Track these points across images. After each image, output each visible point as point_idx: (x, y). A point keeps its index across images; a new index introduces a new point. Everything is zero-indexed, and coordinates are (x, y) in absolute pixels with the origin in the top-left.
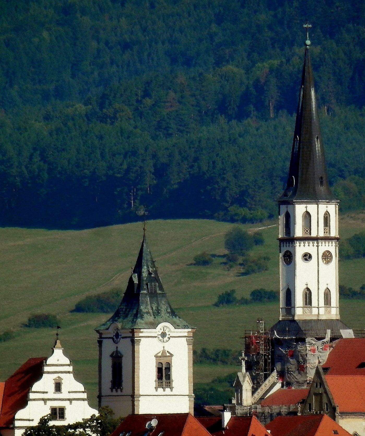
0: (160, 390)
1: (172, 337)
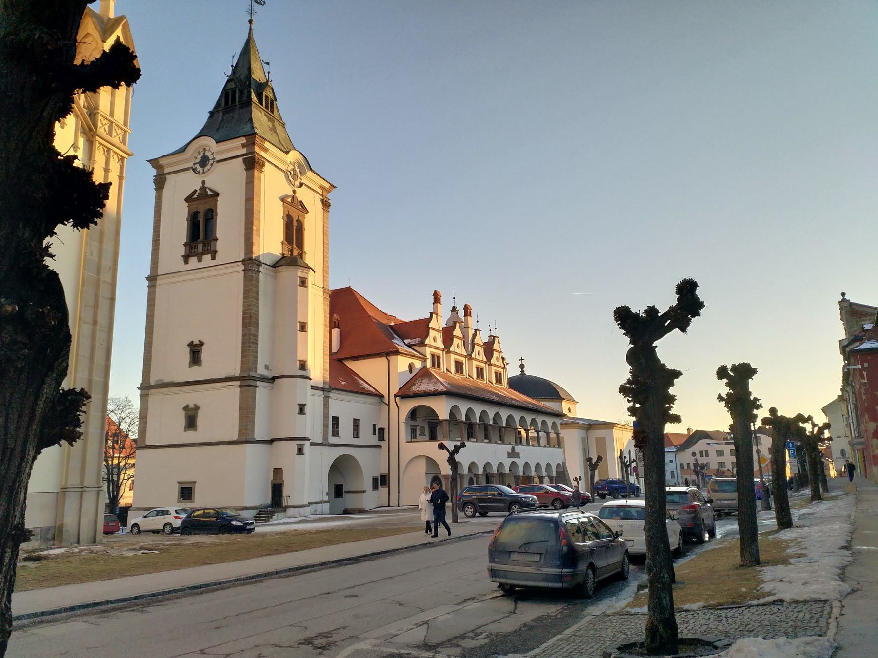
0: (193, 262)
1: (219, 161)
